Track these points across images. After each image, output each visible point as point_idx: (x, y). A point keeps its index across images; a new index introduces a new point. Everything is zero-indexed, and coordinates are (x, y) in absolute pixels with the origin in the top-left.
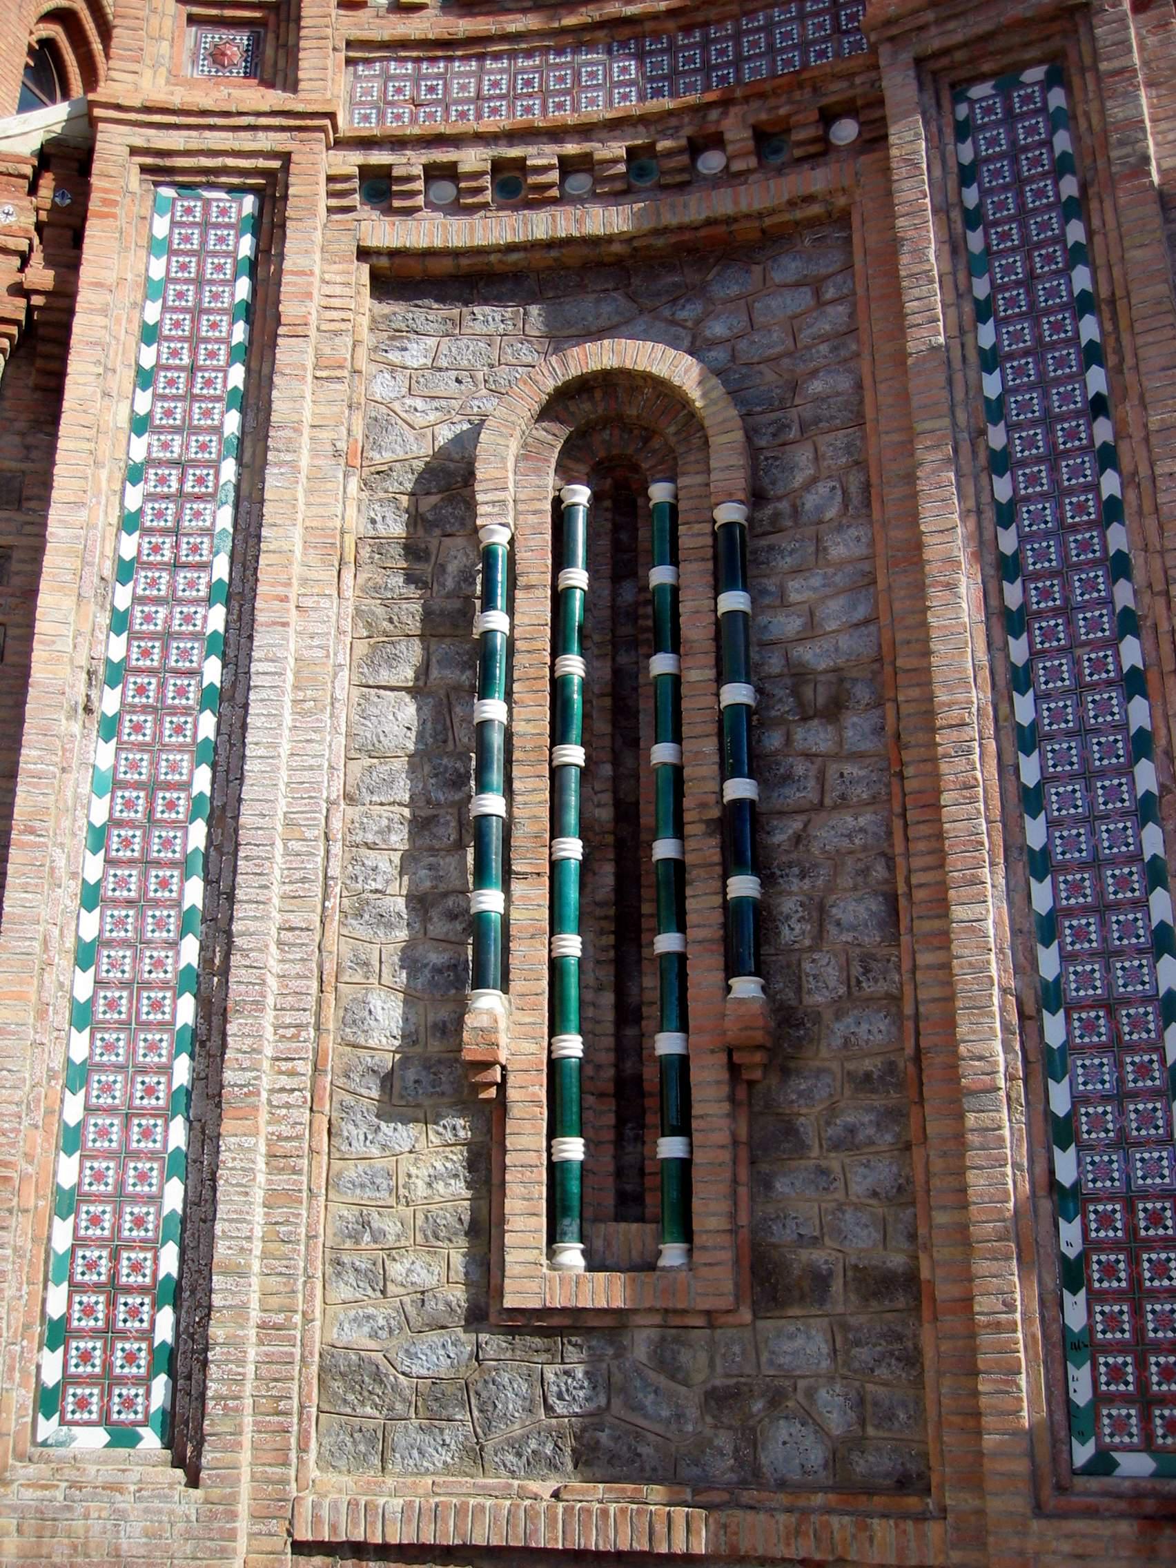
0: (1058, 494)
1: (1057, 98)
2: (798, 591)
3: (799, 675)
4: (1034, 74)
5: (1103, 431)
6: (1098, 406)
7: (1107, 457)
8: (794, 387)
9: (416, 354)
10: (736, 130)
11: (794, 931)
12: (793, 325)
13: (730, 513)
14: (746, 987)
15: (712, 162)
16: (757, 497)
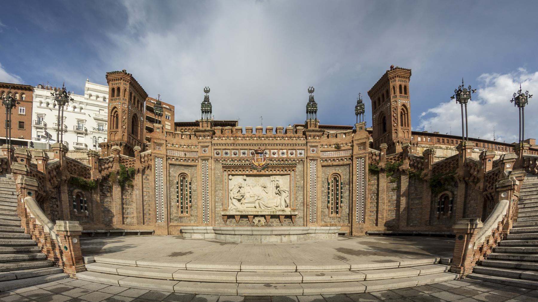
0: (205, 184)
1: (208, 163)
2: (193, 185)
3: (193, 190)
5: (208, 181)
7: (208, 182)
9: (172, 169)
10: (191, 159)
14: (190, 204)
15: (189, 161)
16: (191, 180)
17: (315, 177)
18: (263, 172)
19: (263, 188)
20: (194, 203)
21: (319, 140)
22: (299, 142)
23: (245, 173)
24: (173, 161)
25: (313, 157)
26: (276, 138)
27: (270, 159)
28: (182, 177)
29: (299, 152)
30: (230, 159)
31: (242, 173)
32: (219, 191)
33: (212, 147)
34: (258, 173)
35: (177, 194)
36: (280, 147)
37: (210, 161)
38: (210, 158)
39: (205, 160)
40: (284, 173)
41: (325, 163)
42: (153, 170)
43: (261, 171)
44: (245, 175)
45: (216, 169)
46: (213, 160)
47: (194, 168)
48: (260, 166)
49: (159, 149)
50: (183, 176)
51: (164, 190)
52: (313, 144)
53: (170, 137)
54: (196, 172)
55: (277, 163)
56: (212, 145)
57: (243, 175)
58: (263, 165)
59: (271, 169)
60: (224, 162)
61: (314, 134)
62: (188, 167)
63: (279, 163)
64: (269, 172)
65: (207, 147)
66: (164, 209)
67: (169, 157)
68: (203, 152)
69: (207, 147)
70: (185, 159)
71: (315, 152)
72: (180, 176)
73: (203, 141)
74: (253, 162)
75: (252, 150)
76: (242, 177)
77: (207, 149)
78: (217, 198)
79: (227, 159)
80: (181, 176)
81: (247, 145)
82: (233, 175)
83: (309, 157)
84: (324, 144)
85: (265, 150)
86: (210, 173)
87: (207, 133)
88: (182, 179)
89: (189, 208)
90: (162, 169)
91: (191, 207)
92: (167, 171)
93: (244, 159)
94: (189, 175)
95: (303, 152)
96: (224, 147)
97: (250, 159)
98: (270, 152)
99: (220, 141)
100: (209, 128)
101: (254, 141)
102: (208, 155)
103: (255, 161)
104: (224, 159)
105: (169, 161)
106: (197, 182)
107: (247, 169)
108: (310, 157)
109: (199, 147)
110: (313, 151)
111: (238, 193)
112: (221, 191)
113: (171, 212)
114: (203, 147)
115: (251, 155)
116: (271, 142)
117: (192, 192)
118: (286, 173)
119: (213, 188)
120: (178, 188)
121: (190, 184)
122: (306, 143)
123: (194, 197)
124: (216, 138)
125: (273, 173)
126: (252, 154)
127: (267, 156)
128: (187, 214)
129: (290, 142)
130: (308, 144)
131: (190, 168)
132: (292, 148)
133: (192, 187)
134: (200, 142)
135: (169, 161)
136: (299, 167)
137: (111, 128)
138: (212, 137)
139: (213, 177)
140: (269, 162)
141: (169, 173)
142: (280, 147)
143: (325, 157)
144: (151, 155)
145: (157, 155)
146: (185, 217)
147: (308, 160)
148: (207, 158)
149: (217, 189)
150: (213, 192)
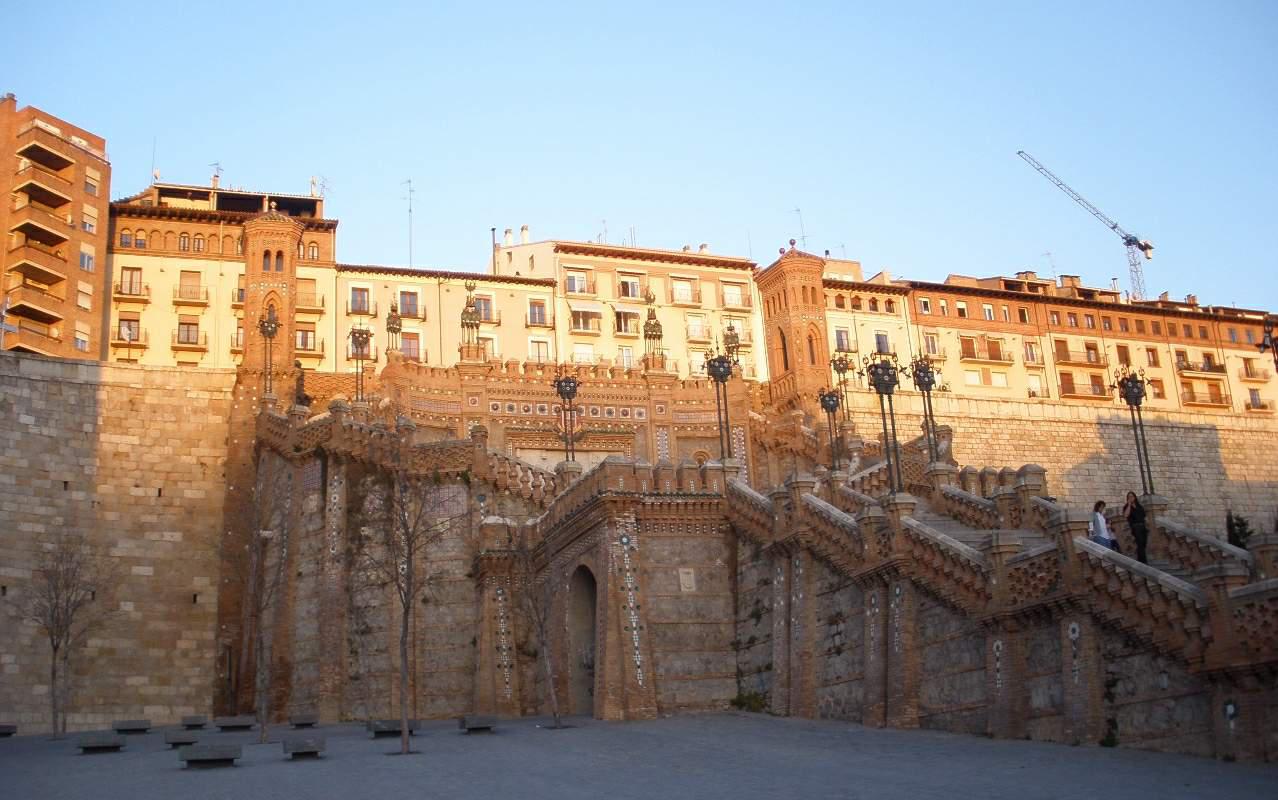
21: (669, 392)
22: (635, 393)
25: (662, 421)
29: (636, 410)
41: (682, 434)
52: (659, 399)
65: (477, 394)
75: (556, 403)
76: (538, 452)
83: (654, 421)
84: (678, 397)
95: (643, 410)
99: (501, 386)
102: (480, 409)
108: (658, 421)
109: (464, 394)
114: (471, 394)
118: (616, 448)
124: (493, 379)
129: (621, 392)
130: (653, 399)
132: (624, 403)
134: (467, 386)
136: (639, 437)
140: (587, 427)
143: (681, 421)
147: (653, 428)
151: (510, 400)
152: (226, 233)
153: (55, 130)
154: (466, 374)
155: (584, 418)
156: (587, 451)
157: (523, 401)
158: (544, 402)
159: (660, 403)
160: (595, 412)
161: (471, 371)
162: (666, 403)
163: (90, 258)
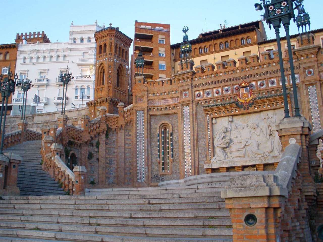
2: (175, 136)
4: (188, 106)
6: (189, 128)
8: (175, 124)
10: (172, 107)
11: (174, 155)
12: (175, 120)
13: (171, 132)
14: (172, 158)
16: (173, 131)
17: (317, 107)
18: (251, 110)
19: (253, 131)
20: (176, 158)
21: (316, 59)
23: (230, 114)
24: (154, 112)
25: (309, 81)
26: (262, 66)
27: (258, 92)
28: (163, 128)
30: (213, 100)
31: (226, 115)
32: (202, 140)
33: (193, 89)
34: (245, 112)
35: (158, 149)
36: (268, 76)
37: (191, 105)
38: (191, 103)
39: (186, 105)
40: (276, 107)
42: (134, 124)
43: (248, 109)
44: (230, 116)
45: (198, 114)
46: (194, 103)
47: (175, 116)
48: (247, 103)
49: (141, 100)
50: (164, 127)
51: (145, 145)
52: (308, 65)
53: (151, 86)
54: (177, 120)
55: (266, 96)
56: (192, 87)
57: (228, 116)
58: (250, 101)
59: (260, 105)
60: (207, 104)
61: (306, 52)
62: (169, 116)
63: (269, 96)
64: (258, 108)
65: (187, 90)
66: (144, 166)
67: (150, 108)
68: (184, 97)
69: (187, 90)
70: (166, 107)
71: (312, 74)
72: (161, 127)
73: (183, 84)
74: (238, 99)
77: (187, 92)
78: (200, 148)
79: (209, 100)
80: (162, 127)
81: (230, 80)
82: (216, 118)
85: (250, 82)
86: (192, 120)
87: (186, 76)
88: (163, 130)
89: (170, 163)
90: (143, 122)
91: (173, 162)
92: (148, 124)
93: (227, 97)
94: (170, 125)
96: (205, 88)
97: (234, 96)
98: (257, 83)
100: (189, 70)
101: (238, 74)
103: (240, 98)
104: (205, 101)
105: (151, 113)
106: (178, 132)
107: (231, 109)
109: (180, 91)
110: (310, 73)
111: (222, 139)
112: (204, 140)
113: (152, 170)
114: (182, 91)
115: (235, 91)
116: (256, 72)
117: (173, 145)
119: (195, 137)
120: (159, 141)
121: (172, 135)
122: (298, 65)
123: (176, 150)
124: (196, 79)
125: (263, 109)
126: (237, 89)
127: (254, 88)
128: (168, 172)
130: (302, 66)
131: (172, 117)
133: (174, 138)
134: (180, 86)
135: (151, 113)
137: (98, 85)
138: (192, 79)
139: (195, 123)
141: (151, 125)
142: (268, 76)
144: (133, 109)
145: (138, 108)
146: (166, 175)
148: (188, 103)
149: (200, 137)
150: (195, 142)
151: (207, 89)
152: (215, 43)
153: (149, 27)
154: (180, 80)
155: (255, 91)
156: (260, 112)
157: (215, 88)
158: (228, 85)
159: (309, 68)
160: (262, 85)
161: (181, 77)
162: (312, 67)
163: (164, 66)
